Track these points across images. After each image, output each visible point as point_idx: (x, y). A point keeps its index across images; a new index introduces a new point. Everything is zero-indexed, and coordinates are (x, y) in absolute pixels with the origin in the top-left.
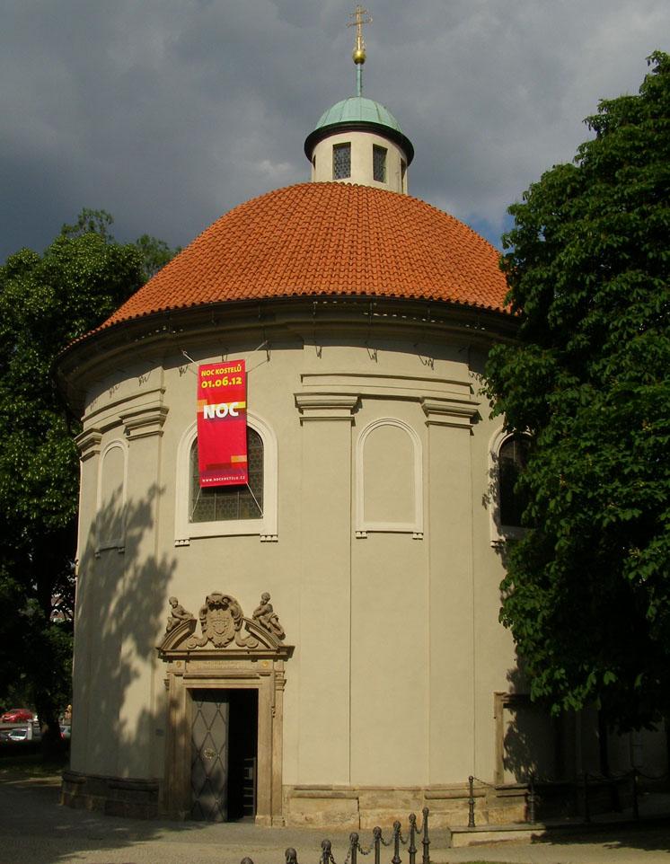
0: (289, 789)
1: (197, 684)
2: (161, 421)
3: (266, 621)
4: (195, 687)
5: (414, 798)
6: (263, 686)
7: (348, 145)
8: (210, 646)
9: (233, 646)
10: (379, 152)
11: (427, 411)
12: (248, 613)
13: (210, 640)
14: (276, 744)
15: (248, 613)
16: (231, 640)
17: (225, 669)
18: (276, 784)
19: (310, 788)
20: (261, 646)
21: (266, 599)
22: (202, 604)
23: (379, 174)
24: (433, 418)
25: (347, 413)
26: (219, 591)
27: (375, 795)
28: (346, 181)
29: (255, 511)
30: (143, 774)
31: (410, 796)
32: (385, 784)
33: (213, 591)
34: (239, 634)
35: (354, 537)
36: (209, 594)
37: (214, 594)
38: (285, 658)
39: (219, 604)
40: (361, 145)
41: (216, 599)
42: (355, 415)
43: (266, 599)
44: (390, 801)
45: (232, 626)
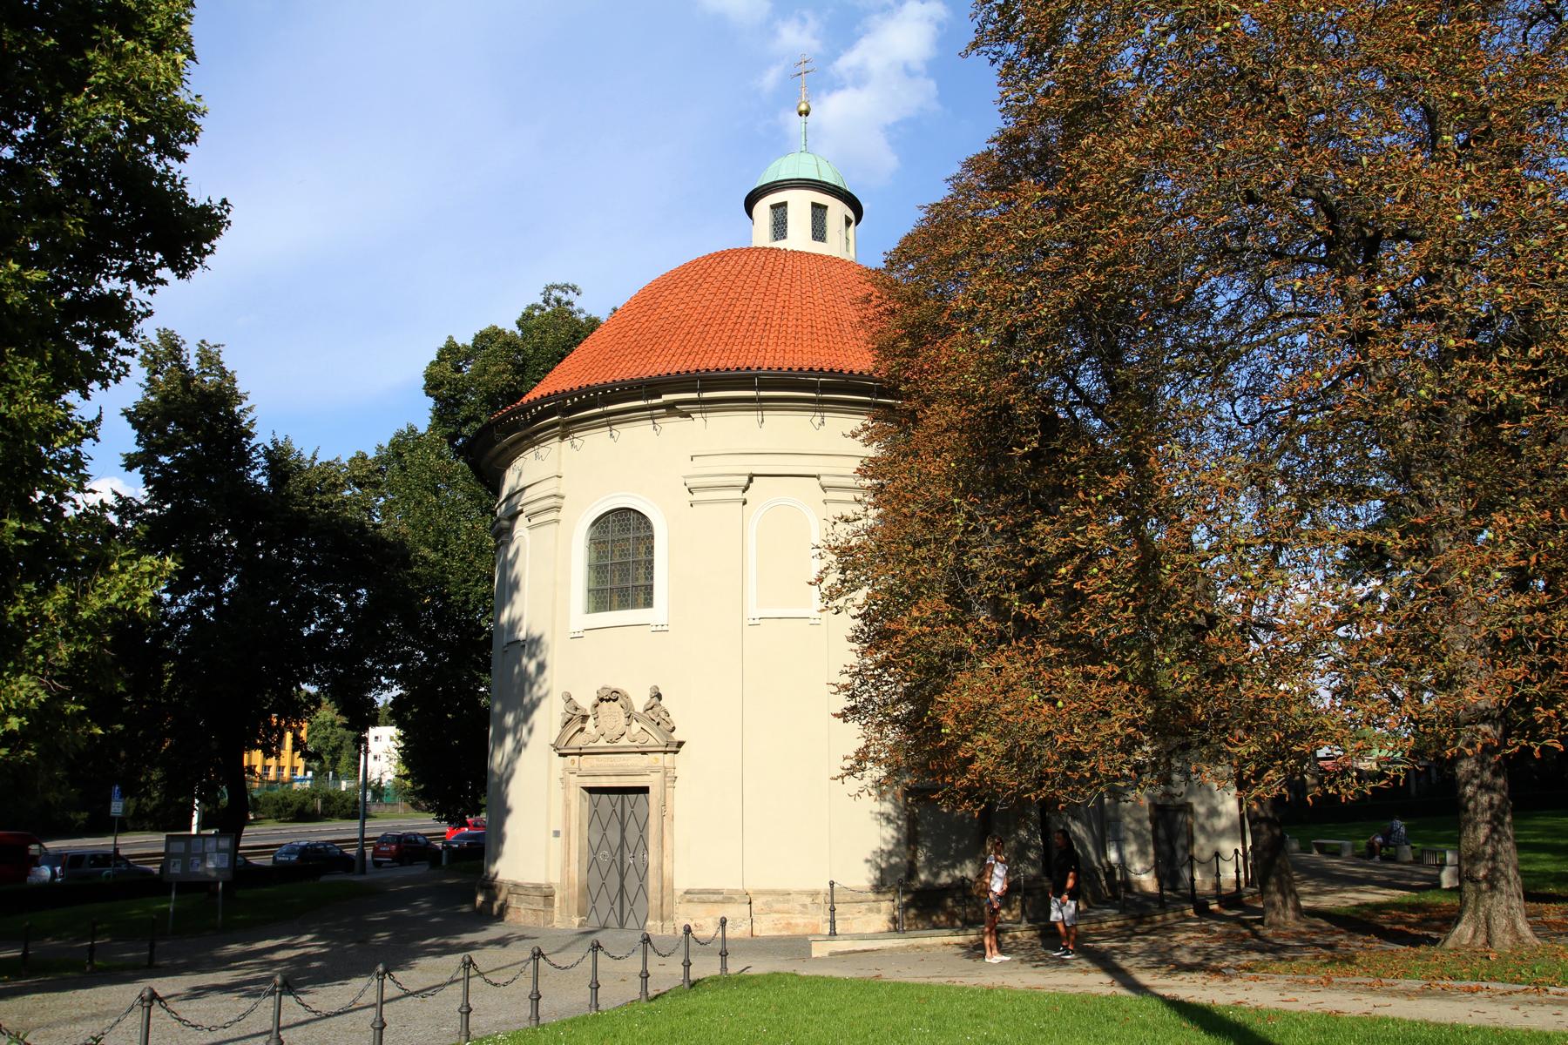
2: (558, 508)
5: (813, 902)
7: (785, 204)
8: (602, 742)
9: (624, 741)
10: (819, 210)
11: (823, 488)
12: (639, 707)
15: (639, 707)
18: (665, 887)
19: (701, 892)
22: (594, 699)
23: (819, 233)
24: (831, 495)
25: (738, 494)
27: (770, 899)
28: (780, 244)
29: (648, 603)
30: (540, 879)
31: (808, 900)
32: (780, 887)
35: (746, 623)
39: (610, 697)
40: (799, 203)
42: (746, 495)
44: (786, 906)
45: (623, 720)
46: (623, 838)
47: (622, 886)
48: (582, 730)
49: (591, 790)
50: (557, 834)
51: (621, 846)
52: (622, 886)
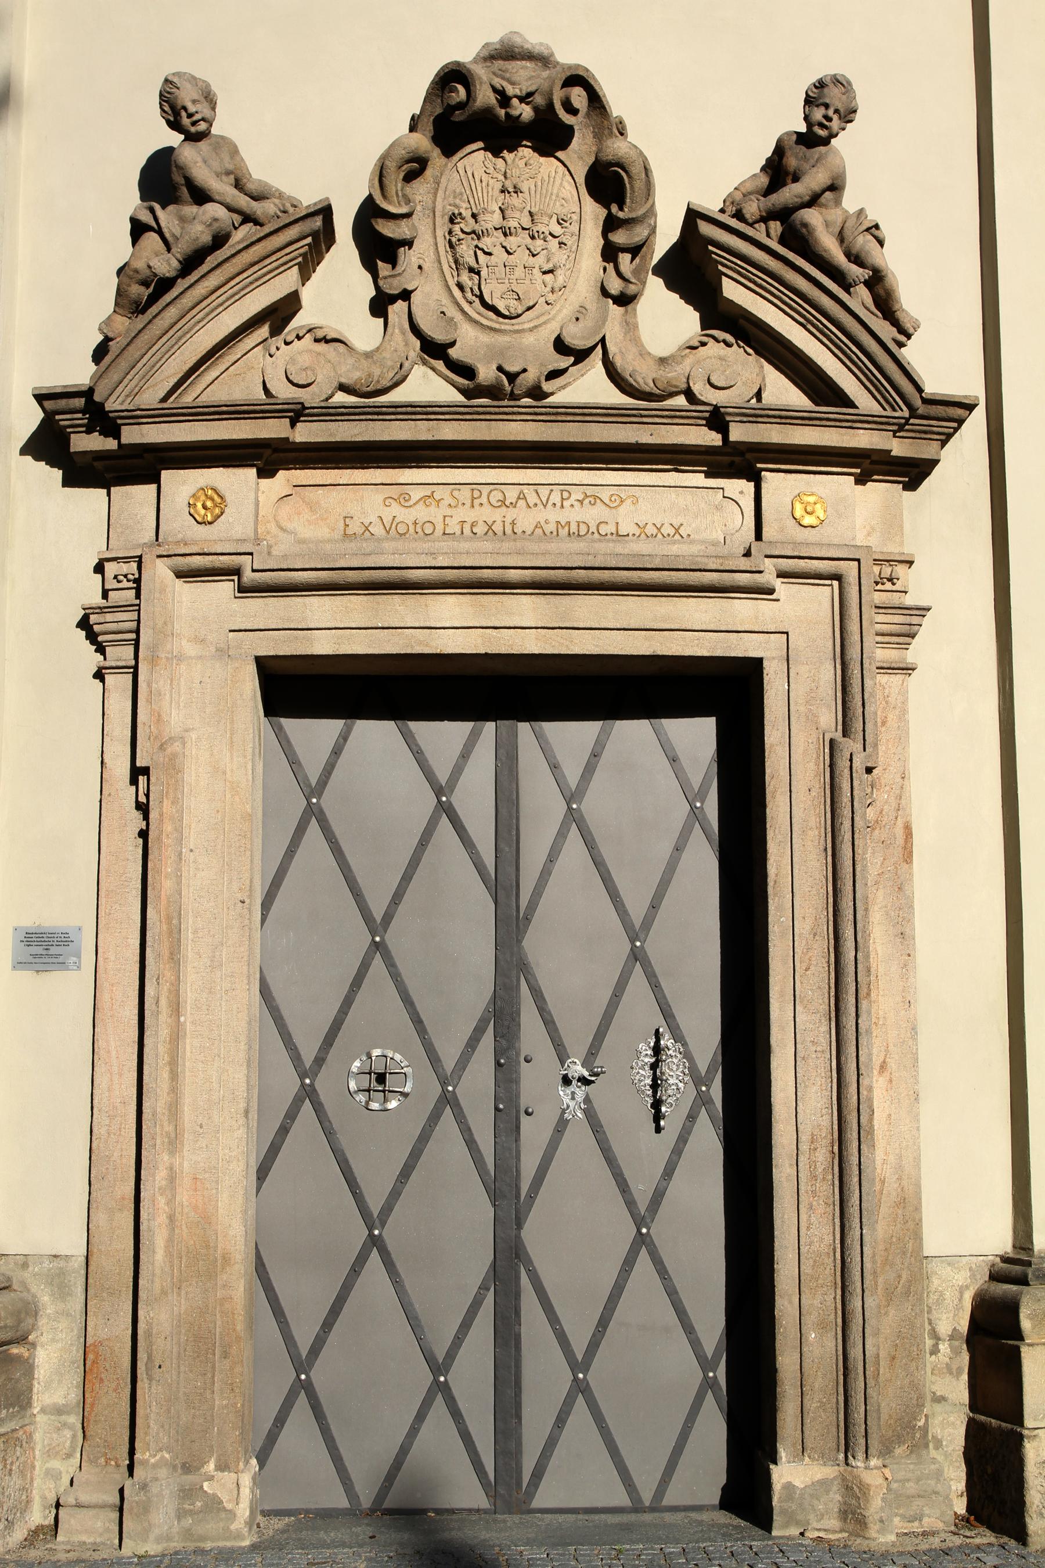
0: (961, 1278)
1: (335, 629)
3: (780, 252)
4: (323, 645)
6: (784, 631)
13: (434, 350)
14: (882, 1005)
16: (581, 356)
17: (540, 534)
20: (783, 391)
21: (827, 108)
26: (533, 38)
33: (494, 37)
34: (630, 327)
36: (465, 53)
37: (506, 53)
38: (913, 473)
41: (523, 77)
43: (827, 108)
46: (511, 965)
47: (509, 1262)
48: (279, 315)
49: (293, 688)
50: (42, 949)
51: (501, 1018)
52: (509, 1262)
